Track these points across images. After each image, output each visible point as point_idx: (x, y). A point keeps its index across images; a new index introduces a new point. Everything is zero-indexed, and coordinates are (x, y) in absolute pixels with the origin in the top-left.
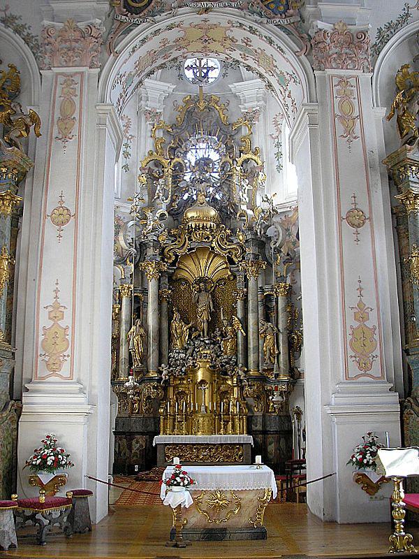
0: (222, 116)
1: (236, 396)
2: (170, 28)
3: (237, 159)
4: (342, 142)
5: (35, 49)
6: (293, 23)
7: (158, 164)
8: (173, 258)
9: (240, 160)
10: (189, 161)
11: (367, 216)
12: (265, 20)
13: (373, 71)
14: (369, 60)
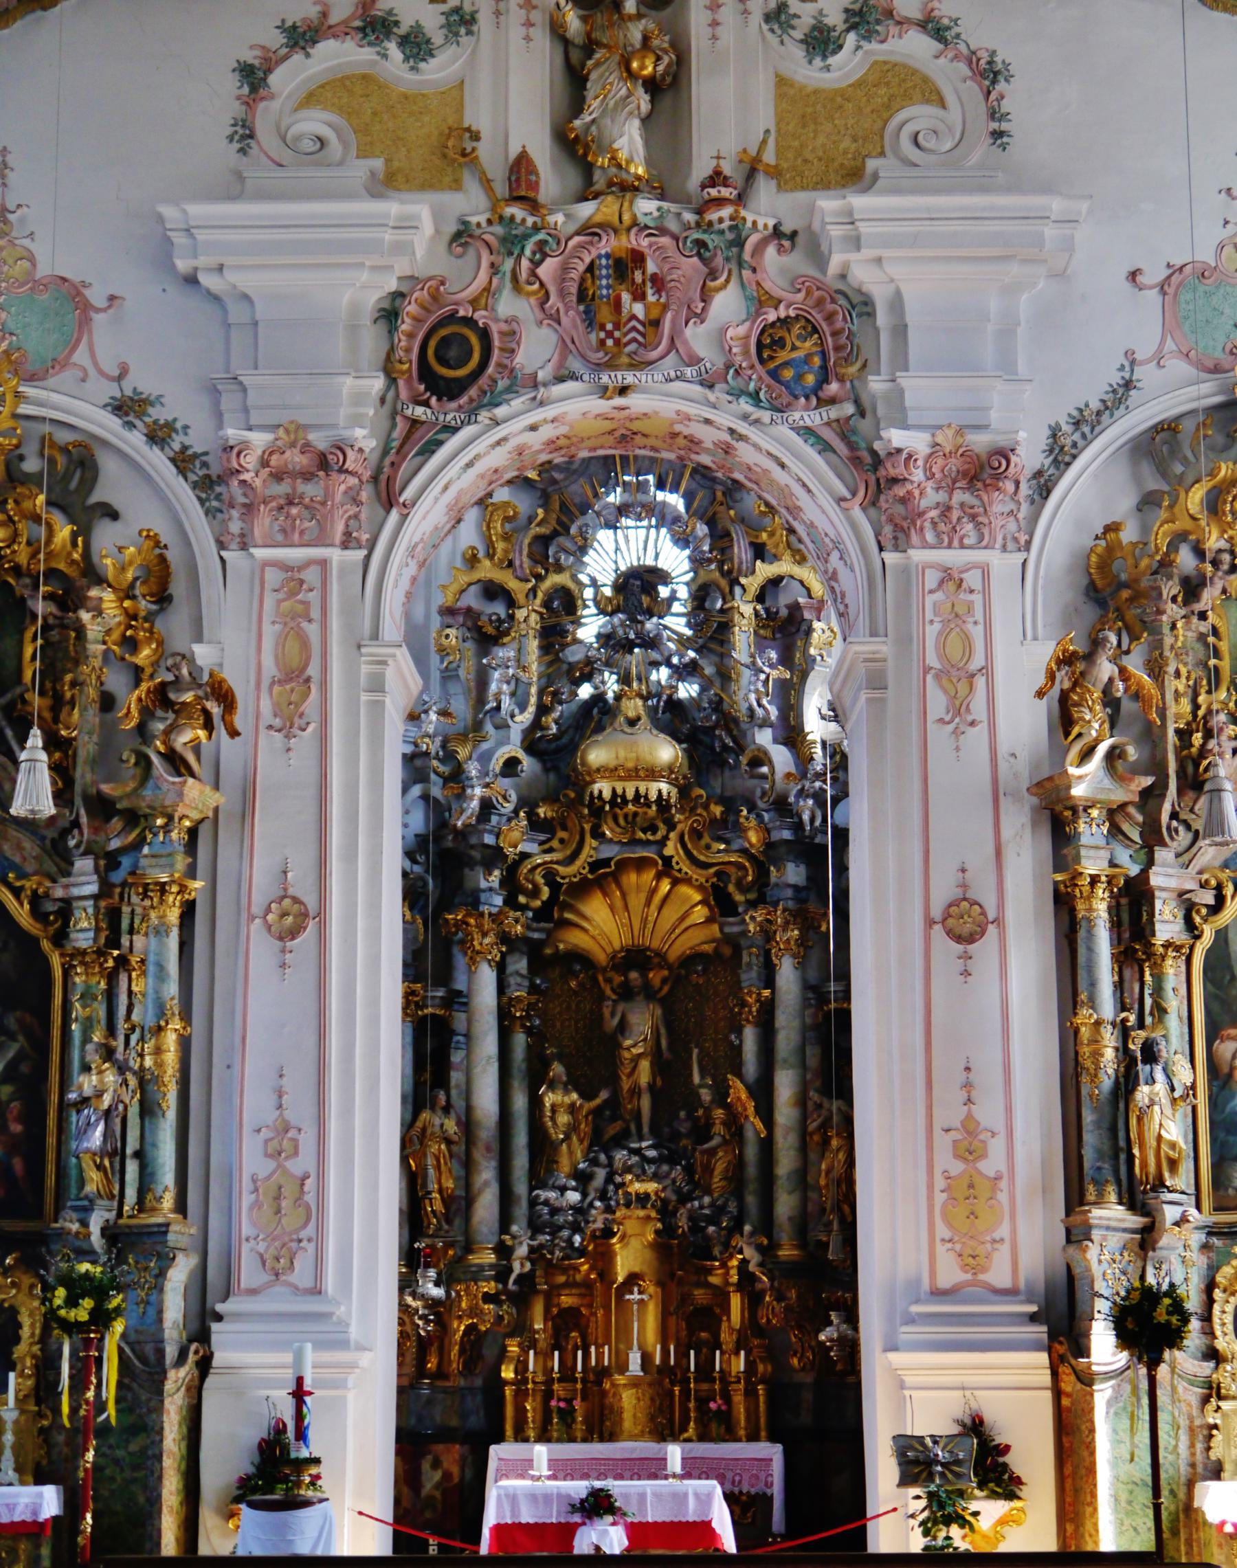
2: (533, 428)
3: (743, 580)
4: (939, 736)
5: (207, 486)
6: (838, 421)
7: (492, 591)
8: (546, 892)
9: (753, 583)
10: (594, 583)
11: (991, 915)
12: (766, 416)
13: (1028, 543)
14: (1021, 516)
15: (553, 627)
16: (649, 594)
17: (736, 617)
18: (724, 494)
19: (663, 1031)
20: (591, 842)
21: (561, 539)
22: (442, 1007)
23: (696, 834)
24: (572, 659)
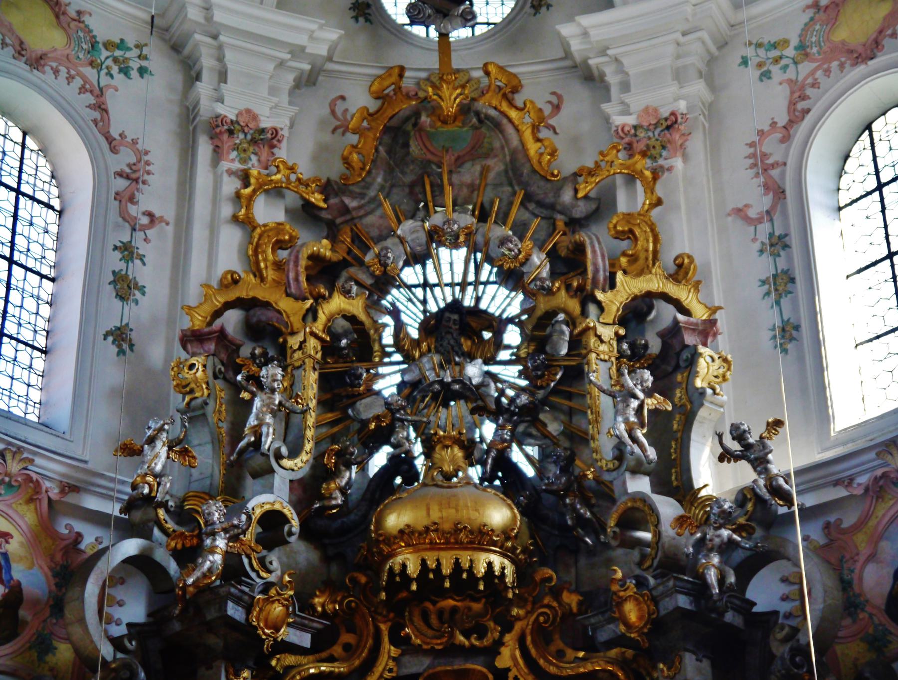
0: (533, 148)
3: (600, 295)
15: (340, 376)
16: (470, 337)
17: (593, 340)
18: (566, 224)
20: (389, 650)
21: (353, 270)
23: (542, 634)
24: (365, 416)
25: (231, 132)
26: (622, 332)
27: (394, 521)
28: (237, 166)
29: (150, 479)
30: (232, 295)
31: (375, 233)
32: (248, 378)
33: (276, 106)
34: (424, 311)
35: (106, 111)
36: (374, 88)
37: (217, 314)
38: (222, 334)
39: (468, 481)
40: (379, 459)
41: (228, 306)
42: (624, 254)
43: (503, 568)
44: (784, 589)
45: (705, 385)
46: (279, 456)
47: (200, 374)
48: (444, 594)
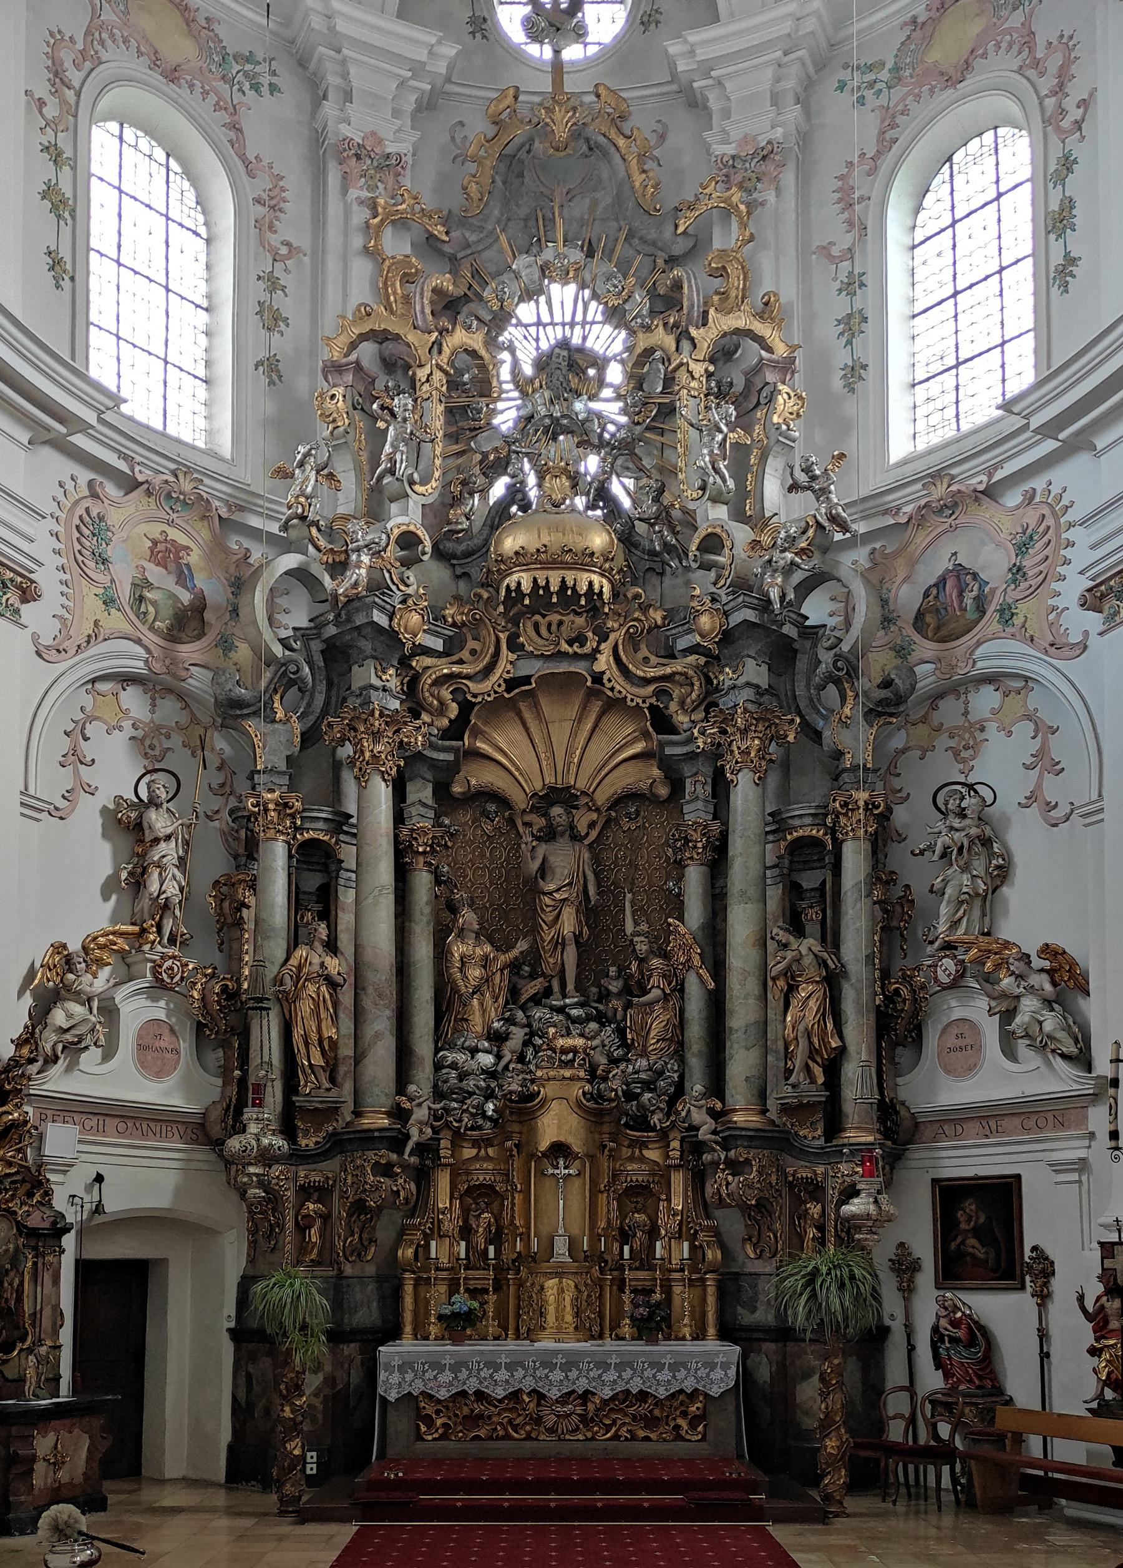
1: (678, 1204)
19: (591, 877)
22: (327, 832)
25: (358, 157)
26: (711, 368)
27: (511, 543)
28: (365, 194)
29: (302, 500)
30: (366, 328)
31: (492, 268)
32: (382, 408)
33: (399, 130)
34: (538, 348)
35: (240, 130)
36: (490, 111)
37: (353, 346)
38: (358, 367)
39: (573, 509)
40: (499, 489)
41: (363, 337)
42: (717, 293)
43: (602, 587)
44: (834, 606)
45: (781, 421)
46: (412, 483)
47: (340, 403)
48: (550, 606)
